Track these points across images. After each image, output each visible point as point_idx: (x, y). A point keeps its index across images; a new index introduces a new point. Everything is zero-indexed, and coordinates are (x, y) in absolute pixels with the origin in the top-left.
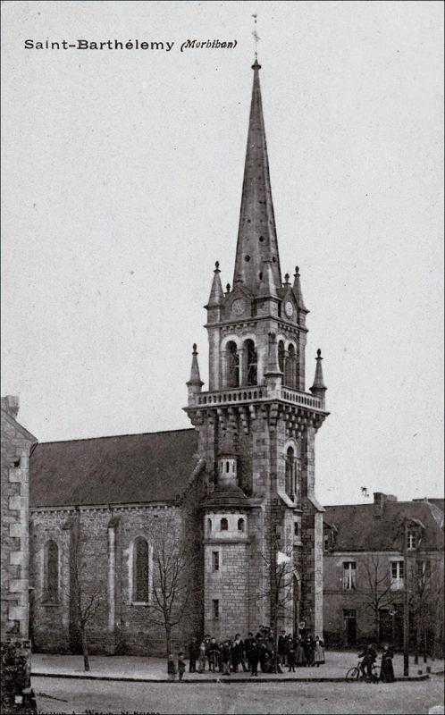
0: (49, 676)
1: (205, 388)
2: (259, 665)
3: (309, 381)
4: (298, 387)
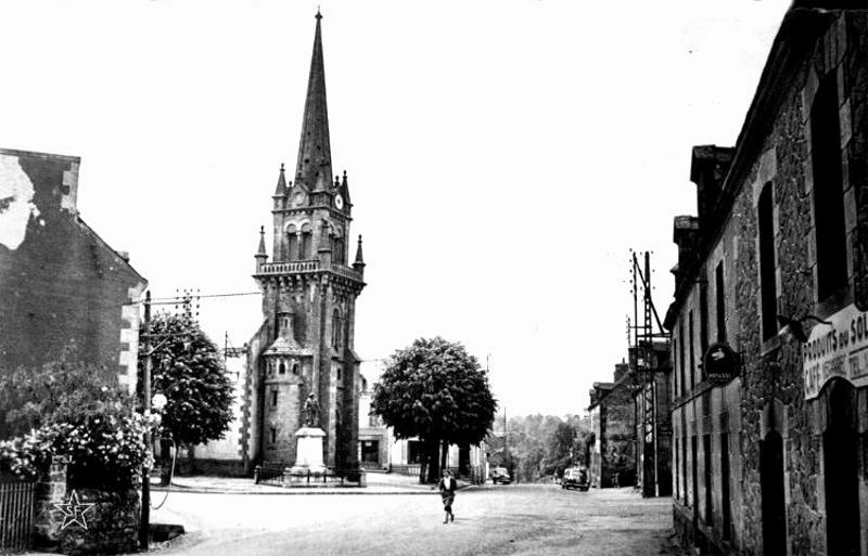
0: (384, 494)
1: (270, 260)
2: (104, 435)
3: (351, 260)
4: (343, 260)
